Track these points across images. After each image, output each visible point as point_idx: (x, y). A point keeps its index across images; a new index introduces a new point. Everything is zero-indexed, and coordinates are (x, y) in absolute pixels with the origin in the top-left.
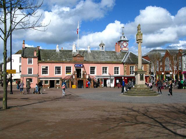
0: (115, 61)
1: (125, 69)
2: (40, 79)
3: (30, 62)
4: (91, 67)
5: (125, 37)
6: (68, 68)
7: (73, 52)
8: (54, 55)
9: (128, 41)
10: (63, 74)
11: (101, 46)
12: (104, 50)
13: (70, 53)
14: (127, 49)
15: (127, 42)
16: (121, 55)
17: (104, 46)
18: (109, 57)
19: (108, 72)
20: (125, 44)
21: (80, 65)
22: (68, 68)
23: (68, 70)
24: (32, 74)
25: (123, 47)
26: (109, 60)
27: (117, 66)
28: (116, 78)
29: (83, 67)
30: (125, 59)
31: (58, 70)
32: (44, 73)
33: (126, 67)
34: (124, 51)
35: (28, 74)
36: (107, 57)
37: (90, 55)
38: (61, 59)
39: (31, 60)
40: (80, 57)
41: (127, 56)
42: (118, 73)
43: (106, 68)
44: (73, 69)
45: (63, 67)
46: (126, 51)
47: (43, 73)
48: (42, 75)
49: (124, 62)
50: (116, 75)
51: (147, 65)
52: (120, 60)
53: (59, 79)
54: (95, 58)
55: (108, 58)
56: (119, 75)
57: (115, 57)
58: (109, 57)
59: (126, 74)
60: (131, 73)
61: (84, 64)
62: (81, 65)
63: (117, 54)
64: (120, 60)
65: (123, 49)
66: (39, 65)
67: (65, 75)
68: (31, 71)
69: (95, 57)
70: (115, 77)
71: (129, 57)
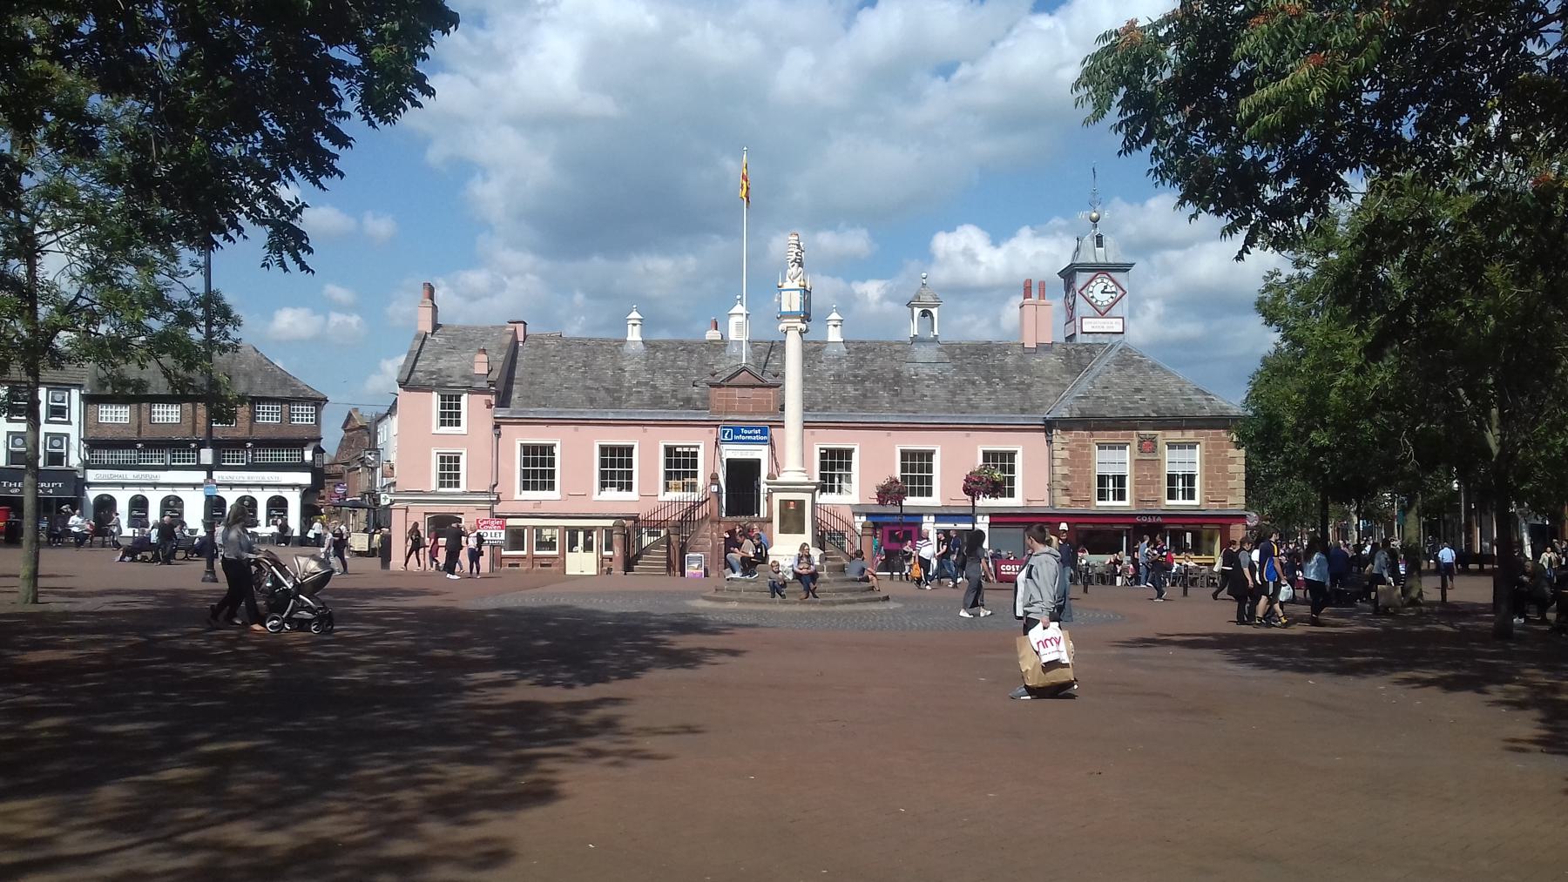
1: (1057, 462)
2: (510, 522)
3: (450, 416)
5: (1107, 240)
9: (1124, 268)
11: (917, 311)
15: (1113, 275)
17: (934, 311)
20: (1099, 290)
24: (463, 487)
31: (616, 468)
35: (434, 484)
40: (753, 386)
42: (1191, 496)
47: (526, 487)
48: (517, 496)
56: (1016, 502)
59: (1066, 500)
66: (499, 436)
67: (661, 498)
68: (457, 468)
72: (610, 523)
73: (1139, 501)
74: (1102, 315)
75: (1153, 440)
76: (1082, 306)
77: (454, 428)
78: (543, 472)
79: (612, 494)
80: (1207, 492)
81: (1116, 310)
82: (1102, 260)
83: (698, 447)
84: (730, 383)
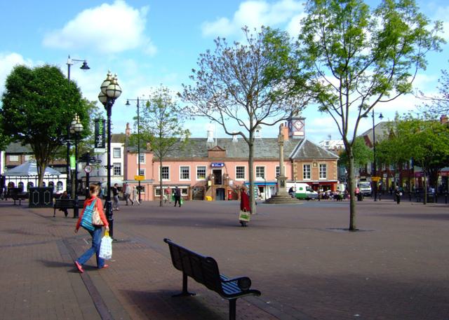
4: (237, 168)
7: (208, 141)
10: (195, 179)
13: (203, 143)
14: (302, 133)
15: (303, 121)
18: (268, 149)
19: (265, 176)
23: (201, 173)
26: (268, 155)
30: (295, 151)
31: (186, 174)
34: (296, 138)
37: (237, 146)
38: (189, 154)
41: (300, 147)
43: (263, 168)
44: (209, 172)
45: (193, 167)
46: (299, 137)
51: (334, 162)
53: (186, 187)
55: (265, 150)
58: (268, 149)
61: (226, 163)
71: (301, 150)
76: (294, 129)
81: (302, 129)
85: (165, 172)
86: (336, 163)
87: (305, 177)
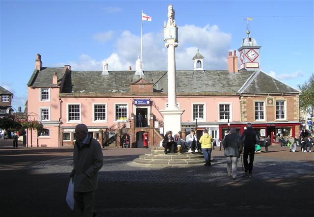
0: (223, 91)
1: (243, 107)
2: (65, 130)
3: (45, 96)
5: (253, 40)
6: (99, 107)
7: (136, 74)
8: (95, 82)
9: (258, 48)
10: (110, 121)
11: (196, 60)
12: (202, 69)
13: (130, 77)
15: (255, 50)
16: (239, 78)
17: (201, 60)
18: (210, 83)
20: (251, 54)
21: (144, 101)
22: (99, 107)
23: (120, 112)
24: (49, 120)
25: (246, 60)
26: (209, 89)
27: (225, 101)
28: (223, 127)
29: (151, 104)
31: (100, 111)
32: (76, 118)
33: (246, 105)
34: (249, 70)
36: (206, 82)
39: (47, 93)
43: (202, 106)
45: (110, 105)
46: (253, 70)
48: (67, 122)
49: (240, 93)
50: (224, 121)
51: (295, 98)
52: (234, 88)
54: (179, 86)
57: (224, 82)
58: (210, 83)
59: (246, 119)
60: (277, 117)
62: (145, 101)
63: (230, 77)
64: (234, 88)
65: (248, 65)
66: (62, 102)
67: (115, 122)
68: (48, 113)
69: (180, 84)
70: (219, 125)
71: (253, 83)
72: (97, 130)
73: (268, 120)
74: (252, 62)
75: (272, 100)
77: (46, 100)
78: (73, 111)
79: (99, 121)
80: (288, 116)
82: (251, 45)
83: (126, 105)
84: (137, 83)
85: (74, 111)
86: (297, 98)
87: (257, 118)
